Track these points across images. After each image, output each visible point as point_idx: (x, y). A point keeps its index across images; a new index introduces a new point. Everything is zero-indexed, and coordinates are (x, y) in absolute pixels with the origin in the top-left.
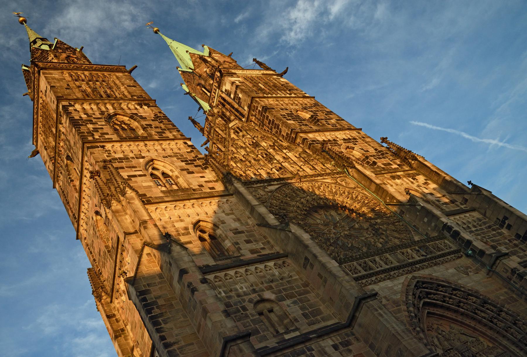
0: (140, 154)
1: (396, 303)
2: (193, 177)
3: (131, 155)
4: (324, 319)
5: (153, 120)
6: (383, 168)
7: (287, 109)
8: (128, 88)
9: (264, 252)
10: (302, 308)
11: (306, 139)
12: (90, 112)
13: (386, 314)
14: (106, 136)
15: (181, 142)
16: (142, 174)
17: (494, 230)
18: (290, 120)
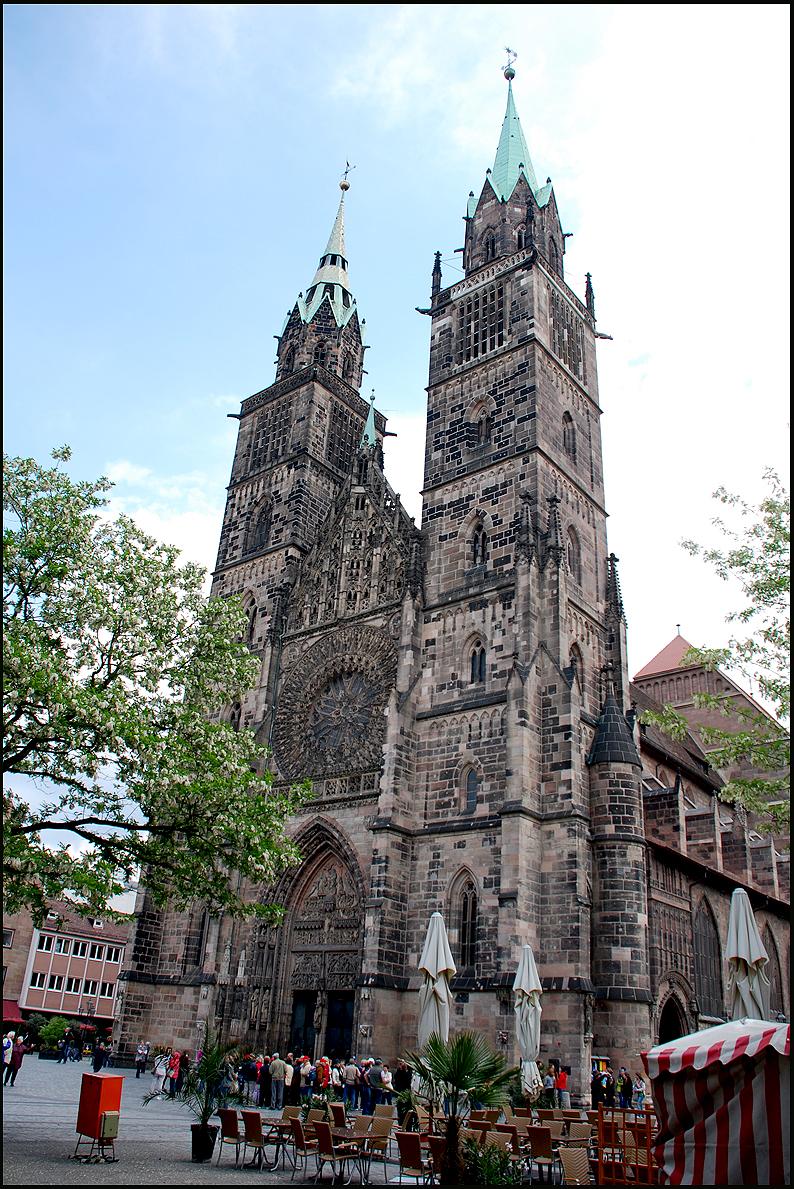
3: (236, 589)
6: (486, 575)
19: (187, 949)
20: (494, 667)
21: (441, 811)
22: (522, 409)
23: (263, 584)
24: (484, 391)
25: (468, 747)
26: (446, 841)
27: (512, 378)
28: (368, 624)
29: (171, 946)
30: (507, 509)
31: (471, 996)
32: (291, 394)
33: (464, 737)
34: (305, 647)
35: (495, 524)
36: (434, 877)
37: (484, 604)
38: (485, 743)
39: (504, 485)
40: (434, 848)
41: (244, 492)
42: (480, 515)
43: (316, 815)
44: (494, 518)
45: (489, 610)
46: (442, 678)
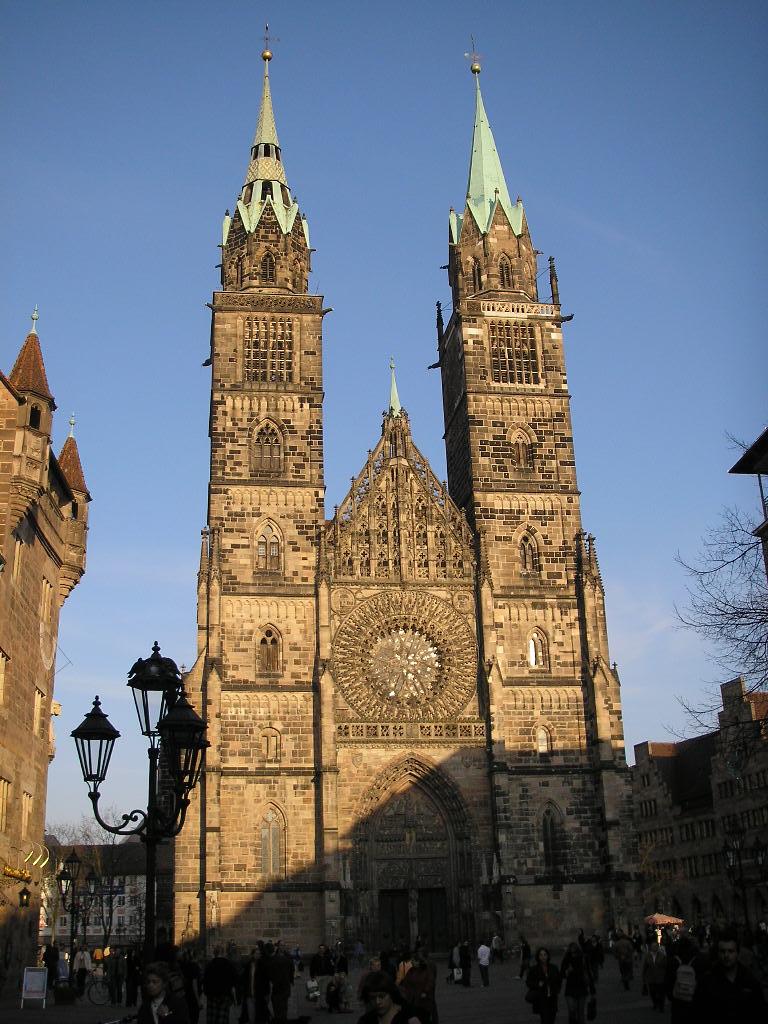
1: (370, 773)
3: (250, 509)
5: (303, 438)
6: (542, 582)
7: (503, 424)
11: (479, 504)
12: (239, 415)
15: (312, 491)
16: (247, 543)
17: (578, 719)
18: (487, 455)
19: (256, 859)
20: (557, 657)
21: (523, 758)
23: (289, 516)
24: (523, 420)
26: (532, 781)
27: (550, 421)
28: (434, 593)
29: (235, 856)
30: (557, 535)
31: (565, 887)
32: (290, 315)
33: (538, 705)
34: (359, 596)
35: (546, 543)
36: (525, 806)
37: (544, 606)
38: (558, 713)
39: (552, 513)
40: (522, 785)
41: (236, 405)
42: (531, 531)
43: (408, 751)
44: (545, 537)
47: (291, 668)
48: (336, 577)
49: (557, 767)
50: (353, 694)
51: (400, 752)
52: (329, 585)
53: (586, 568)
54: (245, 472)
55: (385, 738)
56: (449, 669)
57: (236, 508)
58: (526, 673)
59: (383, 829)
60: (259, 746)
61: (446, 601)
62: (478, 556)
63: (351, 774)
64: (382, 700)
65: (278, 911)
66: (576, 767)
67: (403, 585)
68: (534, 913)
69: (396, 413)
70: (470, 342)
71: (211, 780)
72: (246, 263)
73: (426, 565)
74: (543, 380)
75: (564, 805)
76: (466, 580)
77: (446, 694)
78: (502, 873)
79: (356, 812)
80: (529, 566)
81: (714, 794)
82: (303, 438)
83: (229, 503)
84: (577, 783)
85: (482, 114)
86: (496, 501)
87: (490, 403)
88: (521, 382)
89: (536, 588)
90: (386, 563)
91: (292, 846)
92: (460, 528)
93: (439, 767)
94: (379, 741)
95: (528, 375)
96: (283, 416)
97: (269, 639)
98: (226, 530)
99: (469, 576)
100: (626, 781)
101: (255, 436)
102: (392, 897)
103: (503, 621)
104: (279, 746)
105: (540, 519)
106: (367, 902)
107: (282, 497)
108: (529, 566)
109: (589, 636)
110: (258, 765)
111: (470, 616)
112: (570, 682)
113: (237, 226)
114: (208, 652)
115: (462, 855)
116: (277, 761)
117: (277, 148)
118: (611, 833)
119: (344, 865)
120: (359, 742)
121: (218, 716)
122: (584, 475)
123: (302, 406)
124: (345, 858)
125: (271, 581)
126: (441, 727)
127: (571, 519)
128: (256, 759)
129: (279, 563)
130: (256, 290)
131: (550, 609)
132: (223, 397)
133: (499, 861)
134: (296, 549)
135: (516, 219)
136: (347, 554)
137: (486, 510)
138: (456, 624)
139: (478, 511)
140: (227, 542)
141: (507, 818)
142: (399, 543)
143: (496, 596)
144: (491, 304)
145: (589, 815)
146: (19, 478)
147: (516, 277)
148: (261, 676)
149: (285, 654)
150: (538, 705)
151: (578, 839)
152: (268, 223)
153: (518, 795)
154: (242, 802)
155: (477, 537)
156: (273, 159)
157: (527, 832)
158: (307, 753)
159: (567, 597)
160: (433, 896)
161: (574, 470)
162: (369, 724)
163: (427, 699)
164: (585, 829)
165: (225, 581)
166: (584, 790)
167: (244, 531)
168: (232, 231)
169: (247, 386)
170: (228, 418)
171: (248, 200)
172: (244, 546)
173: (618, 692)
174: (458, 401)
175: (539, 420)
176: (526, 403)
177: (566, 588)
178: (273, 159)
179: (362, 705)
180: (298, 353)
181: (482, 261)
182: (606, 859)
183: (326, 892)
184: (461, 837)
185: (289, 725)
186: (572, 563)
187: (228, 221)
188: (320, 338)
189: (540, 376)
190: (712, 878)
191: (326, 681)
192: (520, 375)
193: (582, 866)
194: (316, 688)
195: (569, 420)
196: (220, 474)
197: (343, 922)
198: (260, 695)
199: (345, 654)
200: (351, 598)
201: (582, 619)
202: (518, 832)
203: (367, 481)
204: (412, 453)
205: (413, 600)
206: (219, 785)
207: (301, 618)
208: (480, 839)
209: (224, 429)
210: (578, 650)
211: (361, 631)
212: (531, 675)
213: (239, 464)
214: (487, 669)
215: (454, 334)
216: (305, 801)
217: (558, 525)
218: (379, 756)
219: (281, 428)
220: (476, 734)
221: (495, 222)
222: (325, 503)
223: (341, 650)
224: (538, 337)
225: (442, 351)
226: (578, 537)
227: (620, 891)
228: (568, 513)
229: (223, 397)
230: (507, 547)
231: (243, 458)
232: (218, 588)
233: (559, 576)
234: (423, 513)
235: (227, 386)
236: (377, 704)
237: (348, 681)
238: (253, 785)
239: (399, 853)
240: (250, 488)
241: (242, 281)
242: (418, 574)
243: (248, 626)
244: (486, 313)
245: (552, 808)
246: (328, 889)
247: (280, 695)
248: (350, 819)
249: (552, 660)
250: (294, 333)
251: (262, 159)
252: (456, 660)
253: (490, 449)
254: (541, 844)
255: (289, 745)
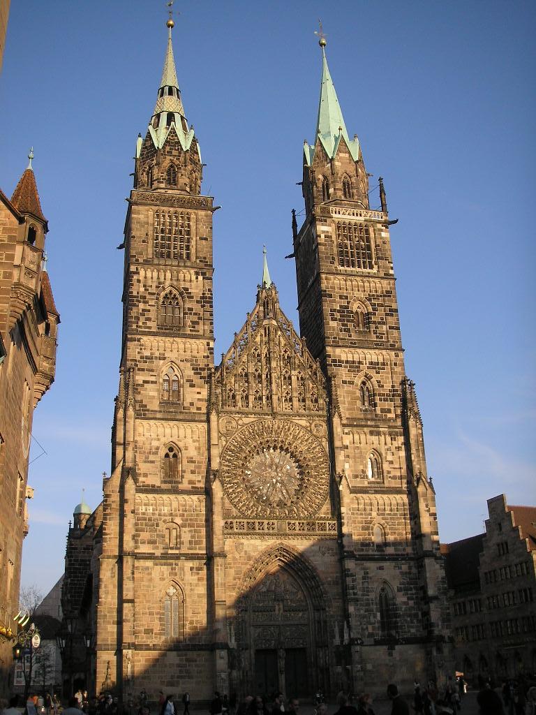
0: (164, 354)
1: (249, 558)
2: (191, 392)
3: (157, 354)
4: (199, 549)
5: (198, 302)
6: (376, 415)
7: (346, 298)
8: (199, 242)
9: (198, 485)
10: (192, 537)
11: (329, 356)
12: (149, 283)
13: (221, 569)
14: (149, 324)
15: (205, 342)
17: (405, 519)
18: (336, 320)
20: (389, 472)
21: (364, 548)
22: (391, 320)
24: (362, 295)
25: (378, 514)
26: (371, 565)
29: (144, 623)
30: (388, 382)
31: (397, 647)
32: (189, 210)
33: (375, 508)
36: (366, 585)
37: (378, 434)
42: (368, 378)
44: (378, 382)
45: (382, 438)
46: (356, 471)
47: (188, 476)
48: (223, 408)
49: (389, 555)
50: (235, 497)
51: (272, 542)
52: (218, 413)
53: (410, 405)
54: (153, 325)
55: (261, 531)
56: (308, 480)
57: (147, 353)
58: (366, 484)
59: (259, 601)
60: (163, 536)
61: (306, 428)
62: (329, 394)
63: (234, 558)
64: (258, 502)
65: (179, 666)
66: (404, 555)
67: (274, 415)
68: (374, 667)
69: (268, 286)
70: (323, 236)
71: (127, 562)
72: (155, 171)
73: (291, 400)
74: (376, 267)
75: (395, 584)
76: (321, 413)
77: (307, 499)
78: (352, 636)
79: (239, 589)
80: (366, 404)
81: (481, 581)
82: (198, 302)
83: (141, 349)
84: (405, 568)
85: (327, 75)
86: (342, 354)
87: (337, 282)
88: (359, 267)
89: (372, 420)
90: (261, 398)
91: (189, 615)
92: (316, 374)
93: (302, 554)
94: (256, 534)
95: (364, 262)
96: (182, 285)
97: (171, 454)
98: (139, 370)
99: (323, 409)
100: (441, 566)
101: (161, 300)
102: (265, 655)
103: (348, 444)
104: (179, 537)
105: (375, 368)
106: (247, 659)
107: (181, 346)
108: (366, 404)
109: (413, 456)
110: (162, 551)
111: (324, 440)
112: (397, 491)
113: (148, 144)
114: (124, 461)
115: (319, 622)
116: (177, 548)
117: (178, 90)
118: (432, 606)
119: (230, 630)
120: (241, 534)
121: (133, 512)
122: (407, 337)
123: (197, 278)
124: (230, 624)
125: (173, 409)
126: (303, 523)
127: (398, 369)
128: (162, 546)
129: (179, 395)
130: (163, 191)
131: (383, 436)
132: (137, 269)
133: (349, 627)
134: (192, 386)
135: (354, 149)
136: (231, 390)
137: (334, 361)
138: (314, 446)
139: (329, 361)
140: (140, 378)
141: (355, 594)
142: (271, 383)
143: (344, 425)
144: (338, 209)
145: (414, 591)
146: (18, 285)
147: (355, 191)
148: (165, 482)
149: (184, 465)
150: (375, 508)
151: (406, 610)
152: (172, 142)
153: (361, 576)
154: (151, 580)
155: (329, 380)
156: (175, 97)
157: (368, 604)
158: (200, 542)
159: (396, 427)
160: (296, 654)
161: (399, 333)
162: (249, 521)
163: (292, 502)
164: (411, 603)
165: (137, 408)
166: (410, 573)
167: (152, 371)
168: (144, 147)
169: (156, 261)
170: (141, 285)
171: (157, 125)
172: (152, 382)
173: (433, 499)
174: (311, 281)
175: (373, 295)
176: (363, 282)
177: (395, 421)
178: (175, 97)
179: (243, 506)
180: (194, 239)
181: (329, 178)
182: (428, 626)
183: (217, 651)
184: (318, 609)
185: (187, 520)
186: (398, 402)
187: (140, 141)
188: (211, 228)
189: (373, 263)
190: (480, 643)
191: (216, 486)
192: (359, 262)
193: (409, 631)
194: (208, 492)
195: (395, 297)
196: (134, 326)
197: (230, 674)
198: (165, 496)
199: (229, 466)
200: (234, 424)
201: (407, 444)
202: (361, 605)
203: (246, 336)
204: (279, 317)
205: (281, 426)
206: (133, 566)
207: (196, 438)
208: (334, 609)
209: (138, 293)
210: (404, 466)
211: (242, 449)
212: (369, 486)
213: (149, 319)
214: (338, 479)
215: (309, 231)
216: (199, 580)
217: (388, 373)
218: (256, 545)
219: (181, 294)
220: (329, 530)
221: (340, 151)
222: (215, 351)
223: (227, 463)
224: (372, 235)
225: (297, 245)
226: (403, 382)
227: (439, 650)
228: (395, 364)
229: (137, 269)
230: (351, 388)
231: (152, 315)
232: (133, 413)
233: (389, 411)
234: (289, 361)
235: (141, 260)
236: (254, 505)
237: (232, 487)
238: (159, 567)
239: (271, 620)
240: (157, 338)
241: (152, 184)
242: (283, 407)
243: (155, 444)
244: (334, 215)
245: (386, 586)
246: (218, 648)
247: (180, 497)
248: (234, 594)
249: (385, 474)
250: (191, 223)
251: (166, 97)
252: (313, 473)
253: (338, 315)
254: (379, 614)
255: (186, 536)
